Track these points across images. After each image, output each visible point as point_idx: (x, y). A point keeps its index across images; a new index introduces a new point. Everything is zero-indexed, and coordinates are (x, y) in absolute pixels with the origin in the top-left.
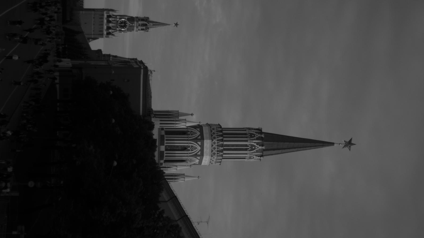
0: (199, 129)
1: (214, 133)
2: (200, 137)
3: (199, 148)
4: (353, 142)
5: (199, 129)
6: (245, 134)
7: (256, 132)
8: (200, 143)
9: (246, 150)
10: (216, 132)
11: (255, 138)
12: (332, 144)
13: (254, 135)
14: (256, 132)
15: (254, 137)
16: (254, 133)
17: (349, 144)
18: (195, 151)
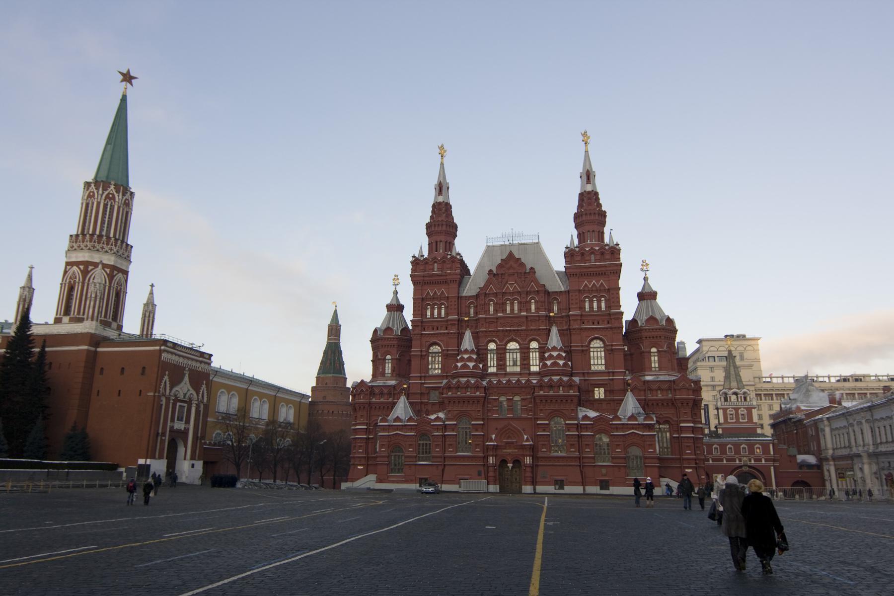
0: (90, 268)
1: (102, 248)
2: (108, 270)
3: (120, 275)
4: (125, 72)
5: (90, 268)
6: (105, 206)
7: (104, 189)
8: (116, 272)
9: (127, 213)
10: (101, 245)
11: (116, 195)
12: (124, 99)
13: (109, 193)
14: (104, 189)
15: (113, 194)
16: (106, 193)
17: (128, 78)
18: (123, 281)
